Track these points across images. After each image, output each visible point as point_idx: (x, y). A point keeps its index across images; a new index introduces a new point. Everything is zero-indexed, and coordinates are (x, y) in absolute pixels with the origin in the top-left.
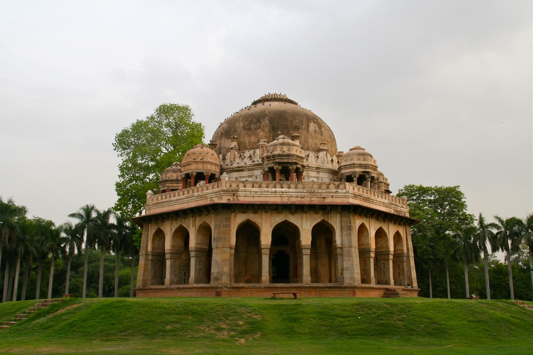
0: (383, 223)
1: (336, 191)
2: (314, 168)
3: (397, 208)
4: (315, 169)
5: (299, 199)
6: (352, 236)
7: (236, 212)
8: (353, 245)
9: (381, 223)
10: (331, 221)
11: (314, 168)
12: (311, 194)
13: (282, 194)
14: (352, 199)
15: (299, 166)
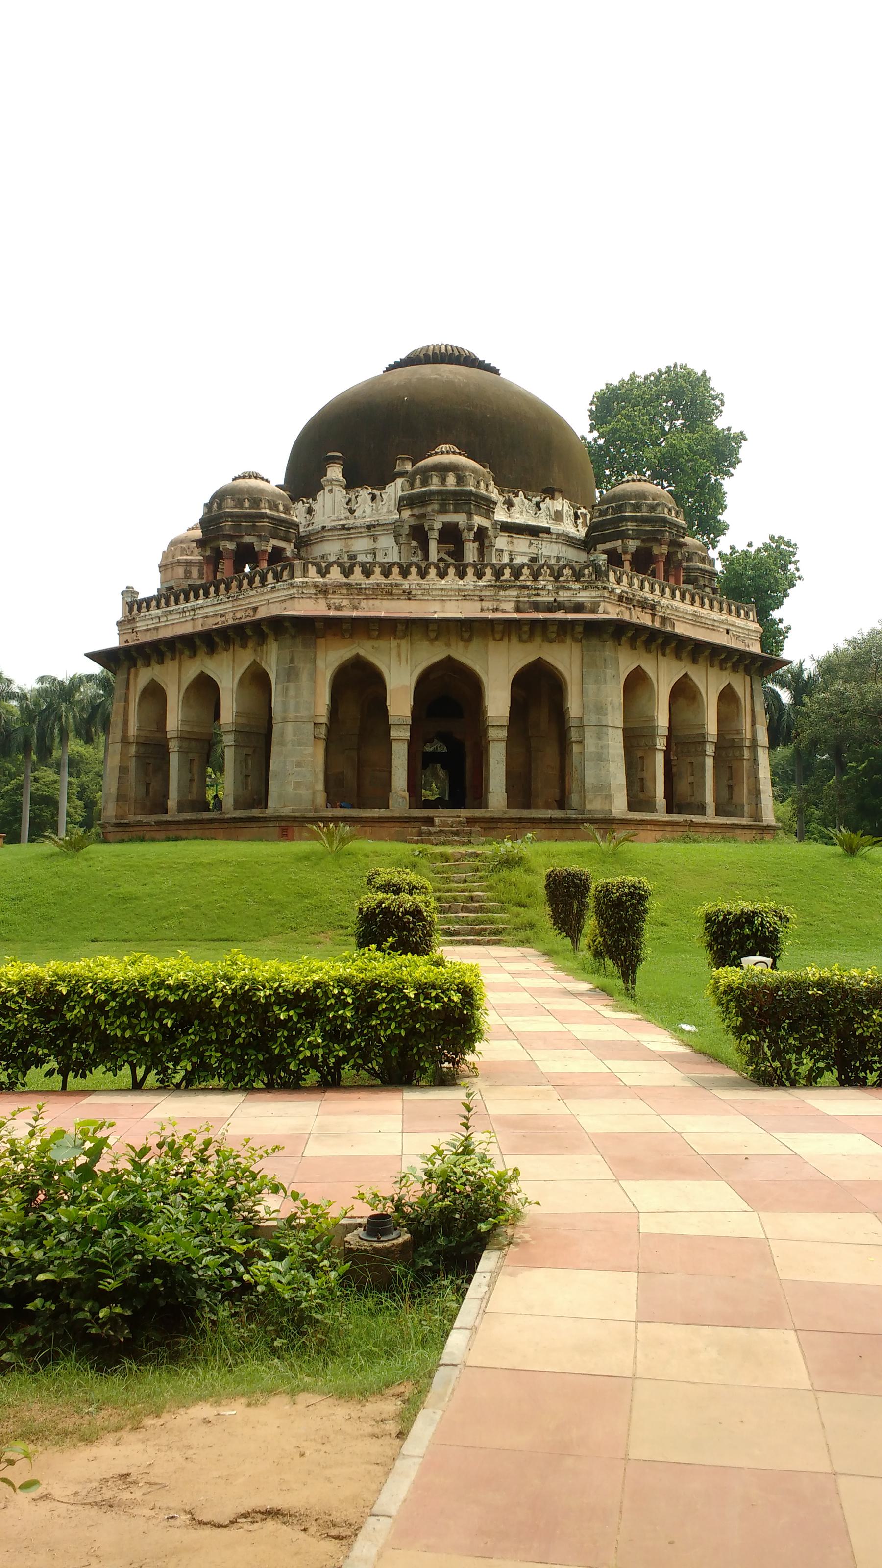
0: (461, 644)
1: (272, 588)
2: (363, 530)
3: (538, 595)
4: (365, 532)
5: (219, 619)
6: (292, 693)
7: (139, 663)
8: (291, 715)
9: (448, 645)
10: (266, 662)
11: (363, 530)
12: (236, 604)
13: (194, 615)
14: (308, 600)
15: (248, 539)
